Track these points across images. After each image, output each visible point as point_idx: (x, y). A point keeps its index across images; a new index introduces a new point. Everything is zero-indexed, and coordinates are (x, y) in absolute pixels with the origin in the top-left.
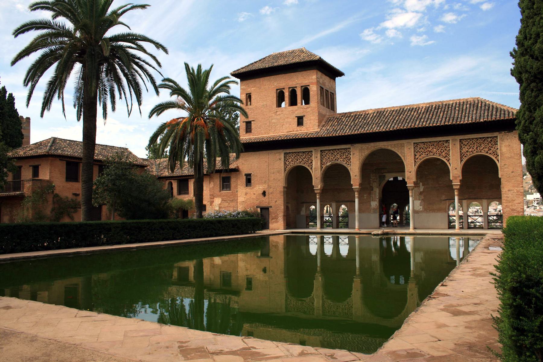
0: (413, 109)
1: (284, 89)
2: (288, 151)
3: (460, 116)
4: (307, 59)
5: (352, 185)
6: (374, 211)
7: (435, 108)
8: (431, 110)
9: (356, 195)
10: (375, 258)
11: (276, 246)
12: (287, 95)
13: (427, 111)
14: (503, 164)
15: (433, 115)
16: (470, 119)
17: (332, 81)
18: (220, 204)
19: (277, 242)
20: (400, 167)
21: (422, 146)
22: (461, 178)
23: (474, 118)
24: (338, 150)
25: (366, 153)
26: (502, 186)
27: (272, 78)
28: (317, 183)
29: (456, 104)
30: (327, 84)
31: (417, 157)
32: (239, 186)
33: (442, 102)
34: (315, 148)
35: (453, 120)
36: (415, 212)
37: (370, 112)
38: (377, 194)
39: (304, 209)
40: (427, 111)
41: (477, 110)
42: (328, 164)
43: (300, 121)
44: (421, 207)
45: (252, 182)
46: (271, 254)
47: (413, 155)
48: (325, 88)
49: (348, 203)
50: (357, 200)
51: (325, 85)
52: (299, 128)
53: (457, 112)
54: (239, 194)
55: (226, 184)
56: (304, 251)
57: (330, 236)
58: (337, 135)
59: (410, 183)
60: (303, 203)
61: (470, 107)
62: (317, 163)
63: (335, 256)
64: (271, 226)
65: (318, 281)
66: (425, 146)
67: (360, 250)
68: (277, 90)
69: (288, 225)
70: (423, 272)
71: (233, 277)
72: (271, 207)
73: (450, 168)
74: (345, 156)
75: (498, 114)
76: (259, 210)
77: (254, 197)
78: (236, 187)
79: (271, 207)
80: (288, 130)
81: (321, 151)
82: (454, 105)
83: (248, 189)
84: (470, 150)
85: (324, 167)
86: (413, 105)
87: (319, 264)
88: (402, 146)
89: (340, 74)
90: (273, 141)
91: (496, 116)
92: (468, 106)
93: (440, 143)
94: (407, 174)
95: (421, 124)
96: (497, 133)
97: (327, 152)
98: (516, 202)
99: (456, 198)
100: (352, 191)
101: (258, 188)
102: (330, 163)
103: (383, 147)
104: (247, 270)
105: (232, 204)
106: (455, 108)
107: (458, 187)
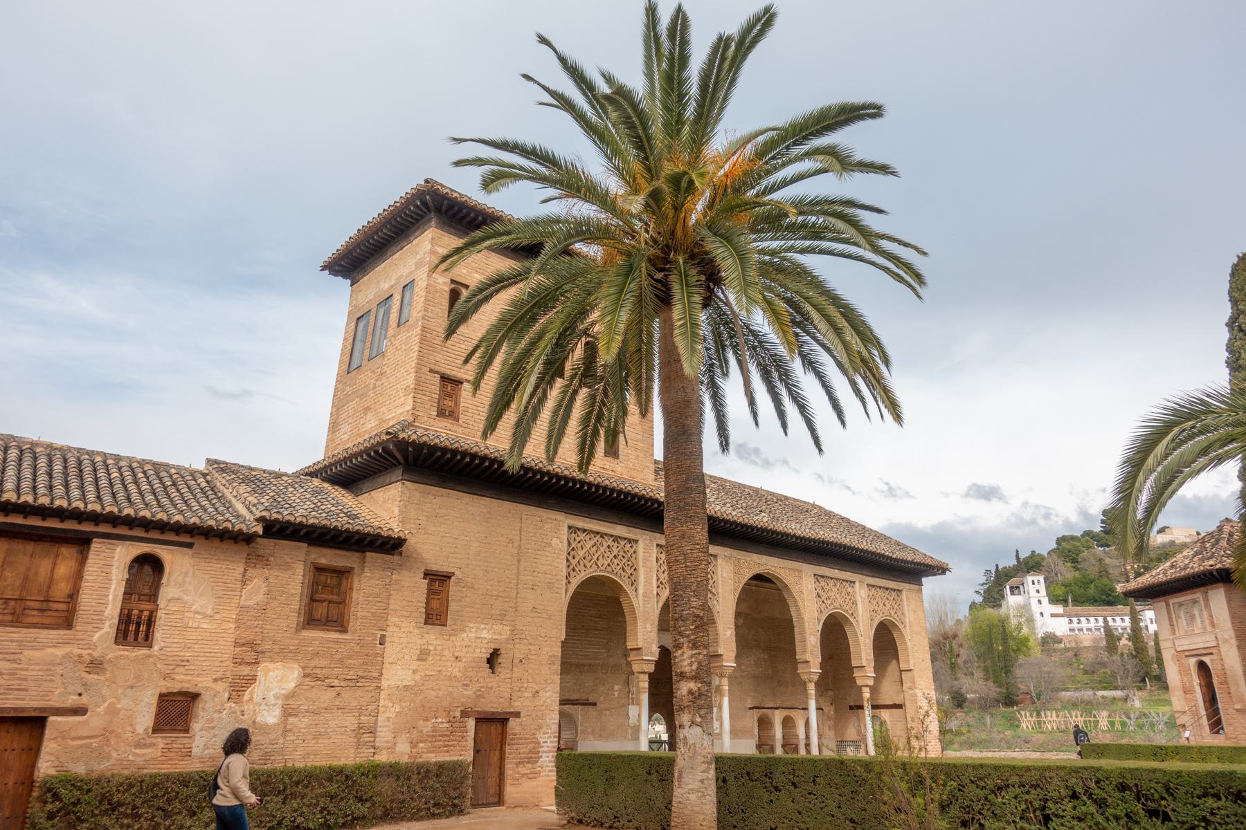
18: (291, 695)
32: (393, 619)
45: (453, 606)
54: (391, 652)
76: (471, 723)
77: (456, 670)
78: (381, 620)
83: (433, 637)
105: (352, 698)
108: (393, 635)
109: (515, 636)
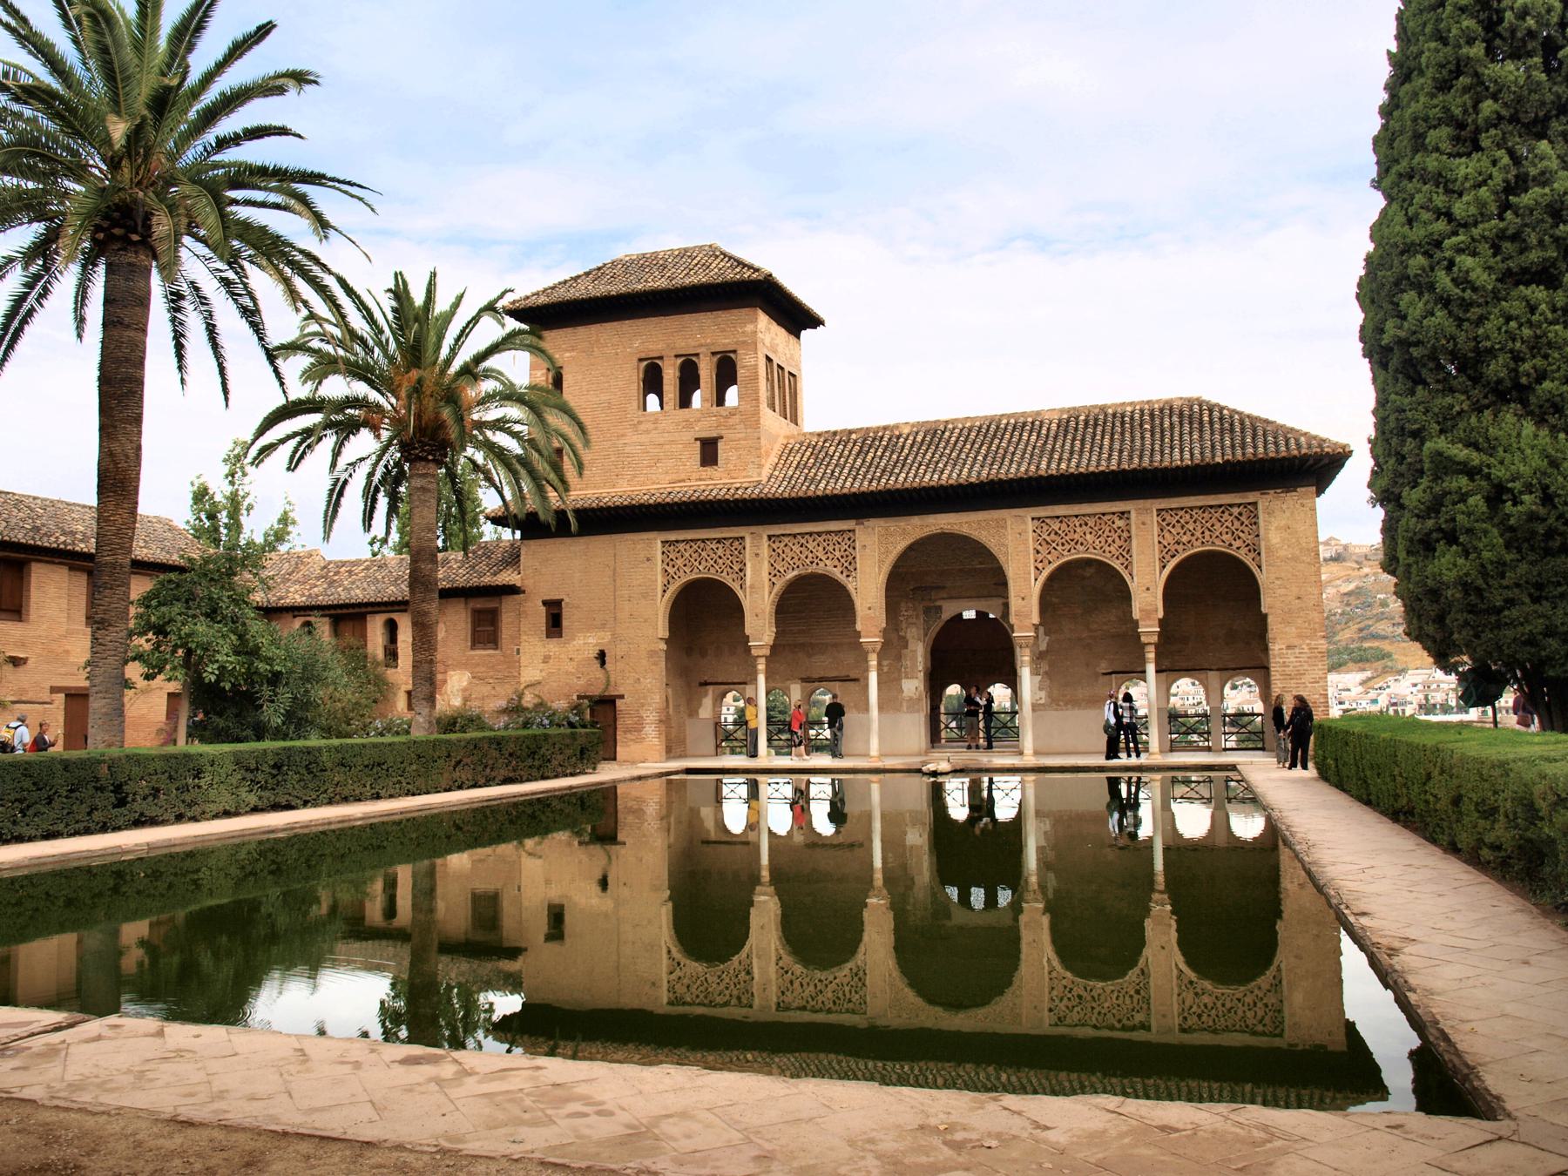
0: (1024, 424)
1: (661, 358)
2: (672, 536)
3: (1157, 447)
4: (730, 275)
5: (858, 635)
6: (912, 704)
7: (1086, 423)
8: (1076, 429)
9: (873, 662)
10: (917, 838)
11: (639, 813)
12: (670, 376)
13: (1066, 431)
14: (1273, 576)
15: (1083, 441)
16: (1187, 456)
17: (792, 338)
18: (464, 690)
19: (638, 799)
20: (994, 580)
21: (1056, 526)
22: (1161, 614)
23: (1196, 452)
24: (819, 534)
25: (901, 546)
26: (1270, 635)
27: (627, 326)
28: (760, 628)
29: (1142, 414)
30: (780, 349)
31: (1040, 557)
33: (1103, 409)
34: (753, 529)
35: (1141, 457)
36: (1035, 707)
37: (906, 431)
38: (920, 659)
39: (708, 702)
40: (1066, 431)
41: (1201, 431)
42: (791, 575)
43: (709, 451)
44: (1043, 694)
45: (565, 623)
46: (620, 837)
47: (1032, 551)
48: (776, 361)
49: (837, 686)
50: (873, 677)
51: (775, 352)
52: (709, 470)
53: (1148, 435)
54: (524, 659)
55: (486, 631)
56: (710, 824)
57: (740, 779)
58: (819, 493)
59: (1021, 629)
60: (706, 684)
61: (1181, 424)
62: (756, 571)
63: (799, 838)
64: (621, 751)
65: (766, 910)
66: (1064, 526)
67: (883, 816)
68: (641, 360)
69: (673, 748)
70: (1051, 875)
71: (507, 906)
72: (622, 697)
73: (1133, 586)
74: (838, 554)
75: (1260, 445)
77: (571, 667)
78: (516, 639)
79: (622, 697)
80: (675, 477)
81: (770, 537)
82: (1137, 416)
83: (553, 646)
84: (1185, 539)
85: (780, 584)
86: (1023, 414)
87: (765, 860)
88: (1001, 525)
89: (814, 322)
90: (631, 508)
91: (1255, 447)
92: (1175, 419)
93: (1105, 518)
94: (1015, 603)
95: (1054, 466)
96: (1257, 494)
97: (786, 540)
98: (1307, 679)
99: (1151, 668)
100: (861, 653)
101: (581, 643)
102: (795, 573)
103: (948, 528)
104: (548, 882)
106: (1141, 425)
107: (1155, 639)
108: (524, 647)
109: (615, 638)
